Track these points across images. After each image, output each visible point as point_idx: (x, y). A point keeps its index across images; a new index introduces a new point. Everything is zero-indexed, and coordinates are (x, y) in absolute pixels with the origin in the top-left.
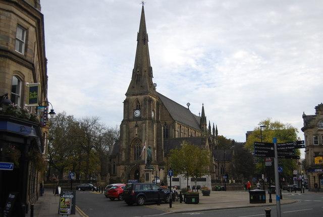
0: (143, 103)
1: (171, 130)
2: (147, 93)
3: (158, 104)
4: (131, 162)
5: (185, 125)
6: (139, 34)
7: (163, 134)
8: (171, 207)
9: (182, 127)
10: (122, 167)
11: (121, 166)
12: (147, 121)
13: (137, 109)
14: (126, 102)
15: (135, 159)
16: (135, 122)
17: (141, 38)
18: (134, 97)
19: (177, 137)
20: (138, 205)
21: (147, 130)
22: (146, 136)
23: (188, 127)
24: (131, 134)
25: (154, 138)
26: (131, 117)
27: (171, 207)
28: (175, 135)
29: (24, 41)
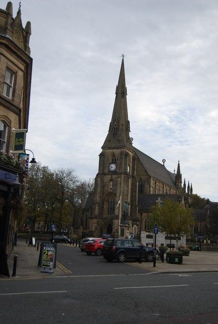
0: (119, 157)
1: (147, 186)
2: (124, 147)
3: (134, 159)
4: (104, 216)
5: (160, 181)
6: (117, 87)
7: (137, 189)
8: (155, 266)
9: (157, 183)
10: (95, 221)
11: (94, 220)
12: (123, 176)
13: (112, 163)
14: (101, 155)
15: (108, 214)
16: (110, 176)
17: (120, 90)
19: (151, 193)
20: (119, 261)
21: (122, 185)
22: (120, 191)
23: (163, 183)
24: (106, 188)
25: (128, 193)
26: (106, 171)
27: (155, 266)
28: (150, 191)
29: (12, 85)
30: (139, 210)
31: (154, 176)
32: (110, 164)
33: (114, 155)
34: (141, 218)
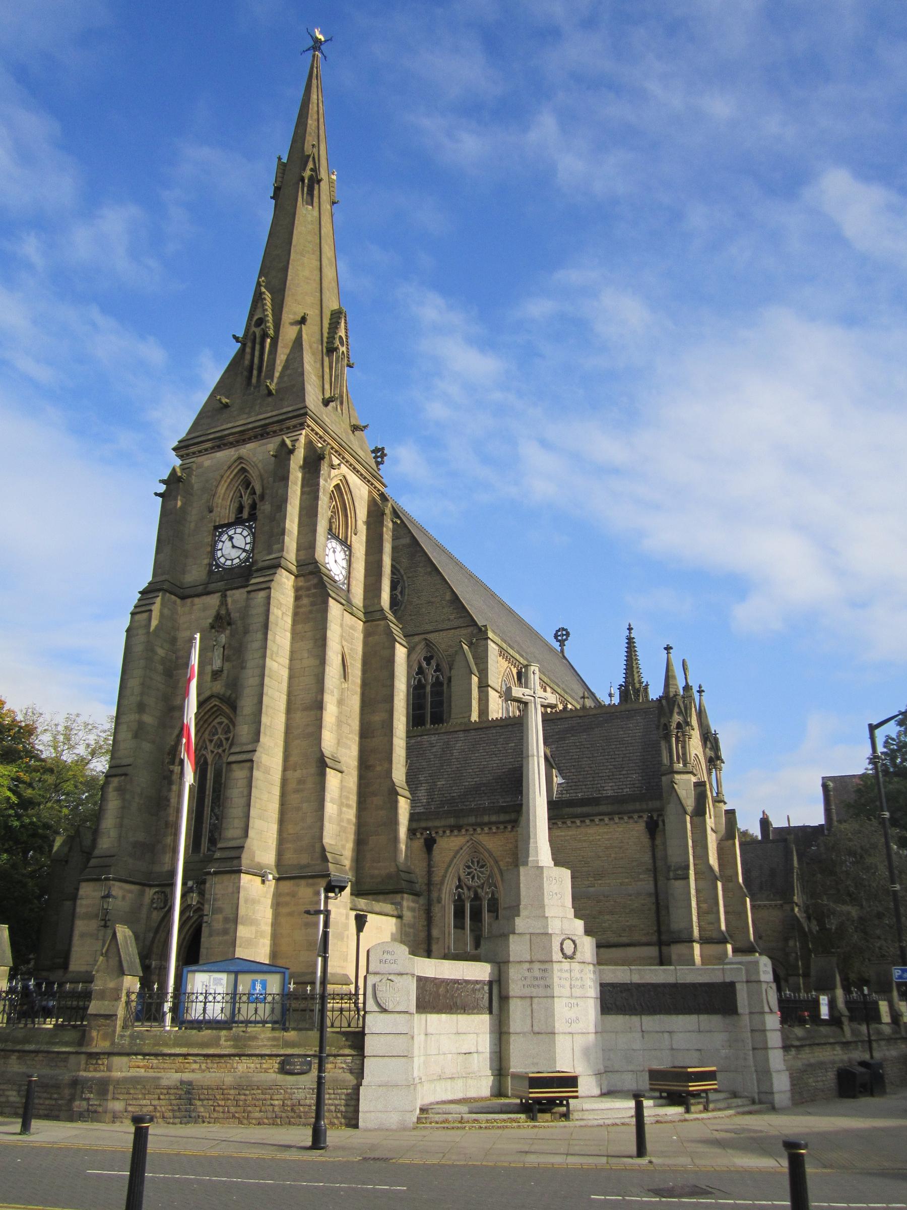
16: (213, 601)
18: (226, 455)
25: (321, 690)
26: (195, 574)
32: (220, 528)
34: (430, 873)
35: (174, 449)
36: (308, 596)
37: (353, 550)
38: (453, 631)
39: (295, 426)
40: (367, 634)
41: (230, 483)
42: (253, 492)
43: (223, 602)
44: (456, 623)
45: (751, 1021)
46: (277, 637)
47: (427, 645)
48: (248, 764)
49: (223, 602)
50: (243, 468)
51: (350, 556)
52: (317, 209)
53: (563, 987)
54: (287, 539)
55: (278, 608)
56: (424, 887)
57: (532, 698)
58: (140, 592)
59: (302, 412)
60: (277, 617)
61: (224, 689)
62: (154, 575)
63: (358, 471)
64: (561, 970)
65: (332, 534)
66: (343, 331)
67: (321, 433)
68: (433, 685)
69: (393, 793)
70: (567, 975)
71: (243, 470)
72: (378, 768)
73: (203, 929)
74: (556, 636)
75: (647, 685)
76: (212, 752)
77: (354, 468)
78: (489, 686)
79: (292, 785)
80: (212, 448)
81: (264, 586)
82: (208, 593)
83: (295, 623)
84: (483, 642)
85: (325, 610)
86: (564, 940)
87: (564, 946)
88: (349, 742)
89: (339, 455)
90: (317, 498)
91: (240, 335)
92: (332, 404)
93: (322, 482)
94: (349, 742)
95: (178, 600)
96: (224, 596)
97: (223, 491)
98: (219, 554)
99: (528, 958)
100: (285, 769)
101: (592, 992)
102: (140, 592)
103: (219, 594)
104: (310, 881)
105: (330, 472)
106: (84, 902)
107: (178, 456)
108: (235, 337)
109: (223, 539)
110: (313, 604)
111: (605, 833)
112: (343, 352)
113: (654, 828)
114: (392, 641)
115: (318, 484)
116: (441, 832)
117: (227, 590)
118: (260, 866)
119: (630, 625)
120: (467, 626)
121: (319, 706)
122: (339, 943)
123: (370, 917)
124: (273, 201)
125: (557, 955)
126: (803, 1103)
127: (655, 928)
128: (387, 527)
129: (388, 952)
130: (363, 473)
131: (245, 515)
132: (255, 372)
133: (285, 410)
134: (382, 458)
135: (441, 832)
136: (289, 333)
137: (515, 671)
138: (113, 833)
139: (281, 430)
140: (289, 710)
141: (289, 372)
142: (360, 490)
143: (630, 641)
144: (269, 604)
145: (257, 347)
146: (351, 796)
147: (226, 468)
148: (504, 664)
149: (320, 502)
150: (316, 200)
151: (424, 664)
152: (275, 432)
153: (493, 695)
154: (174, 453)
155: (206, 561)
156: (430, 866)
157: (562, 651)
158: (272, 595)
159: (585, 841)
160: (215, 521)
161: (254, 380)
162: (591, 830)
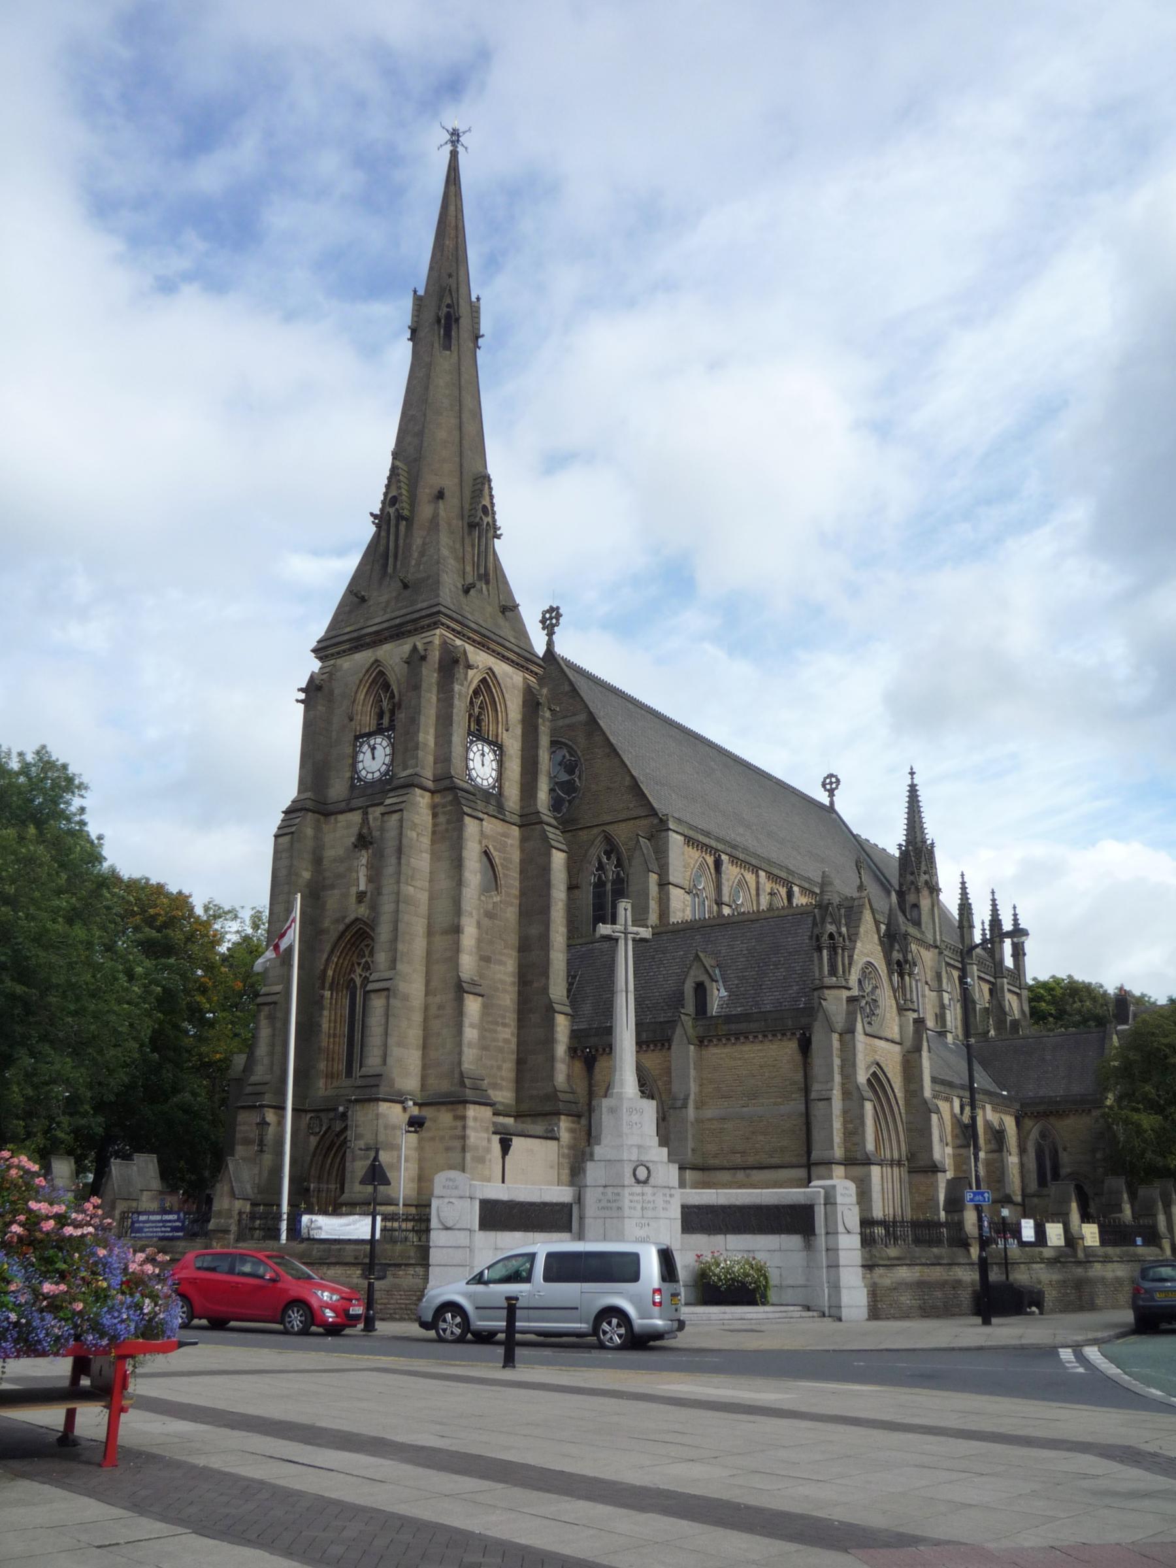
2: (430, 620)
9: (731, 872)
13: (379, 731)
16: (356, 817)
18: (364, 657)
24: (332, 900)
25: (457, 910)
26: (337, 789)
30: (575, 1035)
31: (687, 817)
32: (361, 737)
33: (379, 680)
35: (313, 651)
36: (444, 813)
37: (504, 749)
38: (632, 822)
39: (429, 626)
40: (523, 840)
41: (369, 687)
42: (392, 696)
43: (365, 821)
44: (635, 813)
45: (826, 1242)
46: (412, 860)
47: (606, 837)
48: (385, 993)
49: (365, 821)
50: (380, 671)
51: (501, 755)
52: (455, 355)
53: (635, 1208)
54: (421, 753)
55: (412, 830)
56: (586, 1108)
57: (623, 935)
58: (283, 812)
59: (435, 610)
60: (411, 839)
61: (368, 911)
62: (300, 791)
63: (508, 659)
64: (631, 1194)
65: (478, 734)
66: (488, 498)
67: (459, 629)
68: (614, 882)
69: (550, 1011)
70: (640, 1198)
71: (381, 673)
72: (535, 985)
73: (347, 1154)
74: (824, 785)
75: (932, 844)
76: (361, 975)
77: (503, 656)
78: (669, 884)
79: (433, 1011)
80: (350, 649)
81: (397, 807)
82: (351, 810)
83: (433, 842)
84: (663, 834)
85: (460, 828)
86: (637, 1166)
87: (637, 1173)
88: (504, 959)
89: (483, 646)
90: (451, 706)
91: (377, 512)
92: (472, 592)
93: (457, 687)
94: (504, 959)
95: (322, 818)
96: (366, 814)
97: (362, 697)
98: (360, 766)
99: (604, 1183)
100: (427, 993)
101: (677, 1213)
102: (283, 812)
103: (360, 811)
104: (450, 1107)
105: (466, 674)
106: (243, 1128)
107: (316, 657)
108: (372, 514)
109: (364, 750)
110: (448, 822)
111: (758, 1050)
112: (488, 524)
113: (805, 1046)
114: (547, 847)
115: (453, 690)
116: (601, 1050)
117: (368, 807)
118: (400, 1093)
119: (912, 769)
120: (647, 816)
121: (456, 930)
122: (480, 1166)
123: (517, 1142)
124: (411, 343)
125: (629, 1179)
126: (888, 1318)
127: (805, 1149)
128: (543, 717)
129: (450, 1180)
130: (514, 658)
131: (386, 721)
132: (391, 561)
133: (419, 606)
134: (558, 620)
135: (601, 1050)
136: (425, 511)
137: (710, 860)
138: (266, 1061)
139: (416, 630)
140: (430, 933)
141: (424, 559)
142: (511, 678)
143: (913, 790)
144: (401, 827)
145: (392, 530)
146: (508, 1014)
147: (364, 671)
148: (694, 855)
149: (455, 711)
150: (454, 341)
151: (605, 860)
152: (410, 632)
153: (676, 895)
154: (313, 655)
155: (348, 775)
156: (590, 1086)
157: (832, 803)
158: (405, 817)
159: (740, 1059)
160: (355, 731)
161: (390, 570)
162: (746, 1048)
